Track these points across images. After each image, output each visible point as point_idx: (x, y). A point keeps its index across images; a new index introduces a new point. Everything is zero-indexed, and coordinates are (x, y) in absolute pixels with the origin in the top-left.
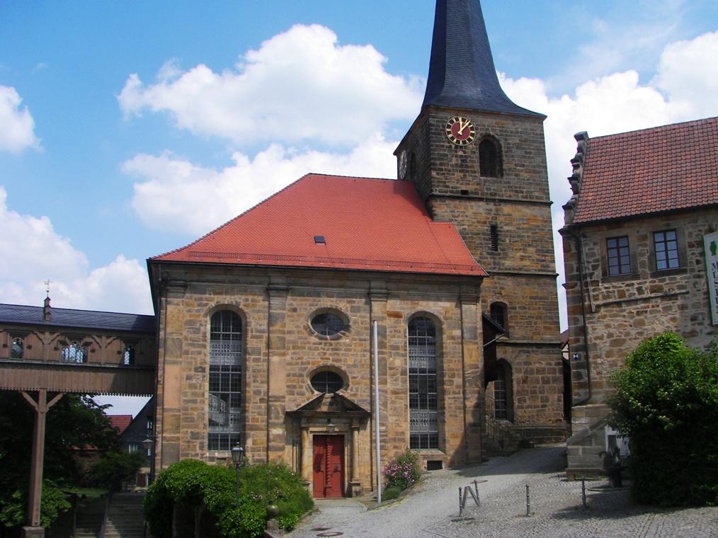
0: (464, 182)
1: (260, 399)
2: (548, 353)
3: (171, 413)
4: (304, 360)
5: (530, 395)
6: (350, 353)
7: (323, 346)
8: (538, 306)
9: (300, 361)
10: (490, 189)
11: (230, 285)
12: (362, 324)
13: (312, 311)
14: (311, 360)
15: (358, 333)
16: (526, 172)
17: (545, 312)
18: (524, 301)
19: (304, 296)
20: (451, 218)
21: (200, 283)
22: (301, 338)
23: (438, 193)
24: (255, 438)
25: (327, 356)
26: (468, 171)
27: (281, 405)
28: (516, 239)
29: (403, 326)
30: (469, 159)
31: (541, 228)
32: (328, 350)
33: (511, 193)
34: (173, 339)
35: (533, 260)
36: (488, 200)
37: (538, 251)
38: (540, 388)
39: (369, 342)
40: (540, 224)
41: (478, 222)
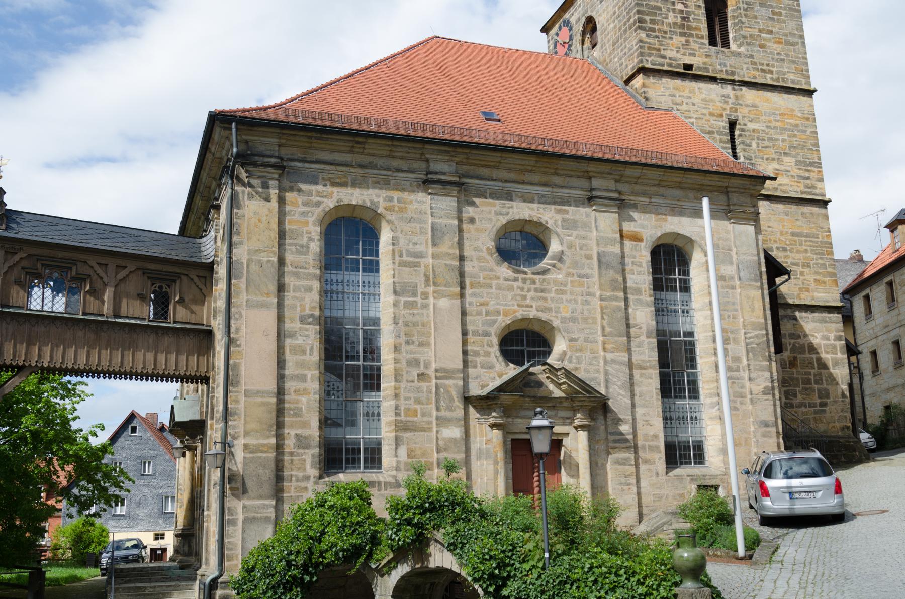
0: (688, 52)
1: (418, 375)
2: (823, 321)
3: (259, 400)
4: (491, 307)
5: (801, 386)
6: (564, 297)
7: (520, 284)
8: (805, 248)
9: (484, 309)
10: (725, 66)
11: (360, 171)
12: (581, 249)
13: (499, 224)
14: (501, 308)
15: (575, 264)
16: (775, 43)
17: (815, 257)
18: (782, 238)
19: (486, 198)
20: (672, 105)
21: (307, 165)
22: (482, 269)
23: (649, 66)
24: (413, 446)
25: (528, 302)
26: (691, 35)
27: (456, 386)
28: (766, 143)
29: (645, 257)
30: (693, 16)
31: (801, 128)
32: (529, 290)
33: (757, 74)
34: (260, 260)
35: (792, 176)
36: (724, 81)
37: (798, 163)
38: (815, 375)
39: (596, 279)
40: (798, 122)
41: (711, 114)
